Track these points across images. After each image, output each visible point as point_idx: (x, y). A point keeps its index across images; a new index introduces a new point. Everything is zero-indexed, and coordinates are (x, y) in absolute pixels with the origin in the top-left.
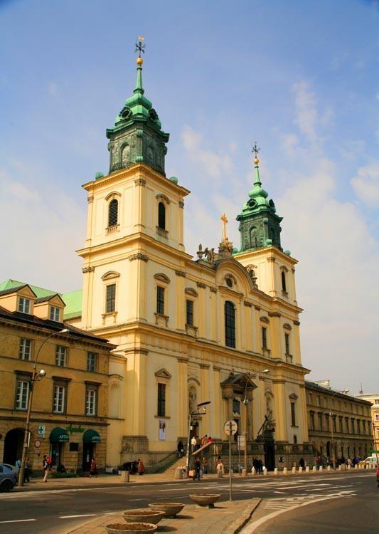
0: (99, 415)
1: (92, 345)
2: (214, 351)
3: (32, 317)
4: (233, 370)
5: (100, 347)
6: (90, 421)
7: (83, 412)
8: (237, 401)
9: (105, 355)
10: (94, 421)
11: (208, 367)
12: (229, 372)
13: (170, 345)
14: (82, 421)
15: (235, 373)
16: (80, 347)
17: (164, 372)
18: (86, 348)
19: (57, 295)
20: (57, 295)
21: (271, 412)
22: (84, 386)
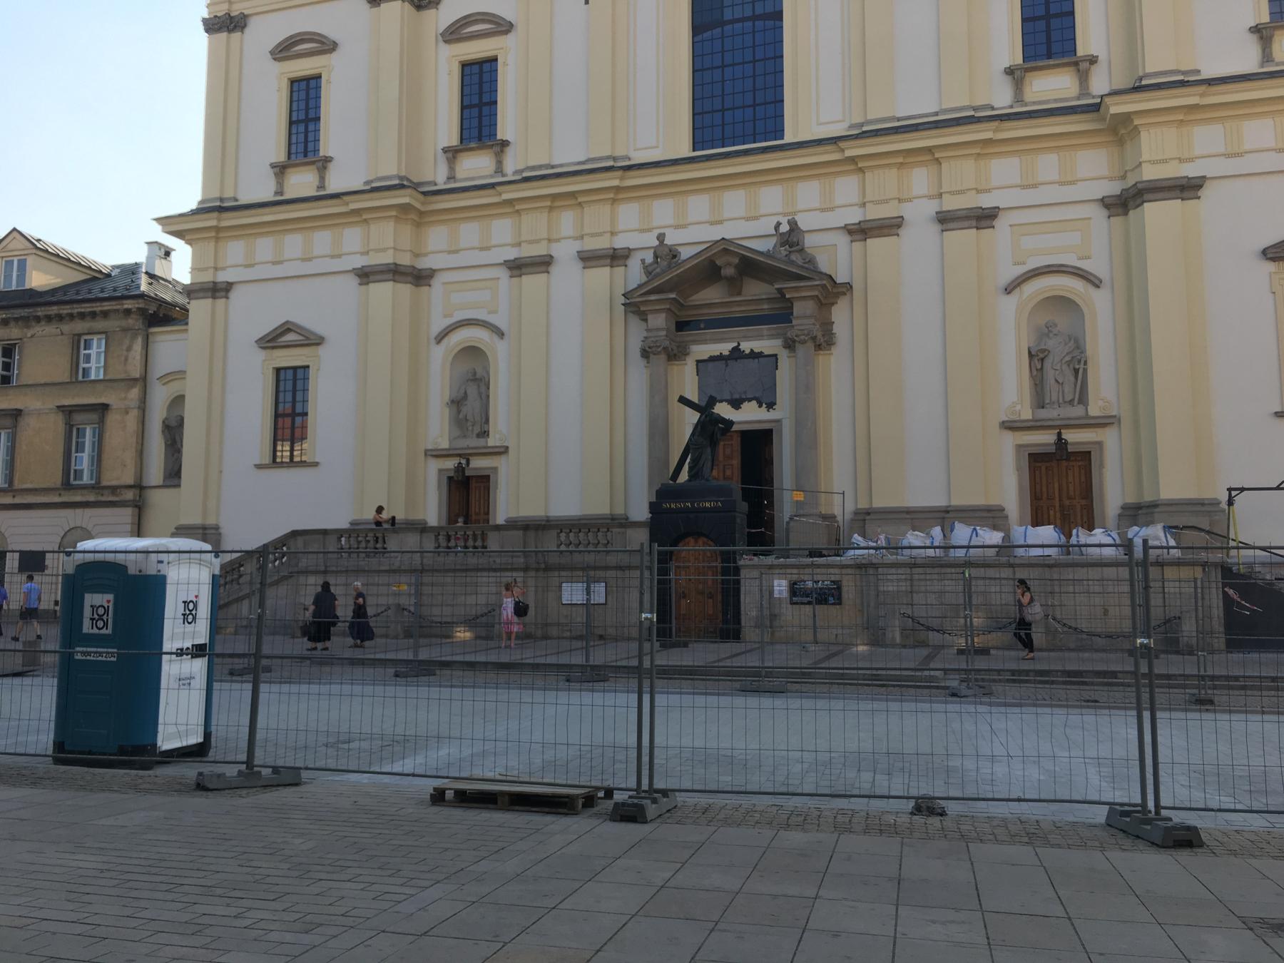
0: (104, 483)
1: (82, 316)
2: (573, 195)
3: (32, 293)
4: (661, 237)
5: (105, 314)
6: (78, 498)
7: (57, 480)
8: (754, 355)
9: (125, 330)
10: (92, 498)
11: (544, 263)
12: (649, 258)
13: (322, 240)
14: (57, 499)
15: (685, 253)
16: (50, 329)
17: (289, 330)
18: (66, 328)
19: (15, 229)
20: (15, 229)
21: (1078, 367)
22: (58, 422)
